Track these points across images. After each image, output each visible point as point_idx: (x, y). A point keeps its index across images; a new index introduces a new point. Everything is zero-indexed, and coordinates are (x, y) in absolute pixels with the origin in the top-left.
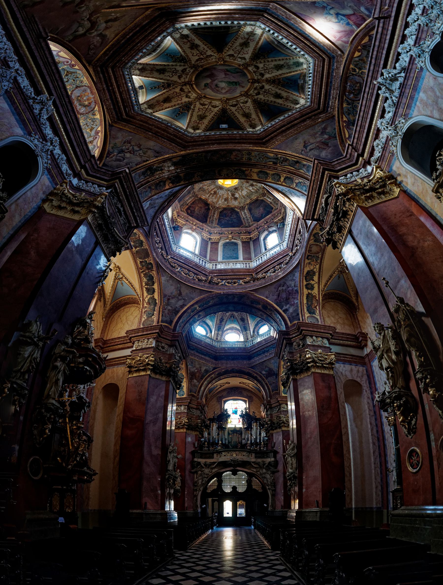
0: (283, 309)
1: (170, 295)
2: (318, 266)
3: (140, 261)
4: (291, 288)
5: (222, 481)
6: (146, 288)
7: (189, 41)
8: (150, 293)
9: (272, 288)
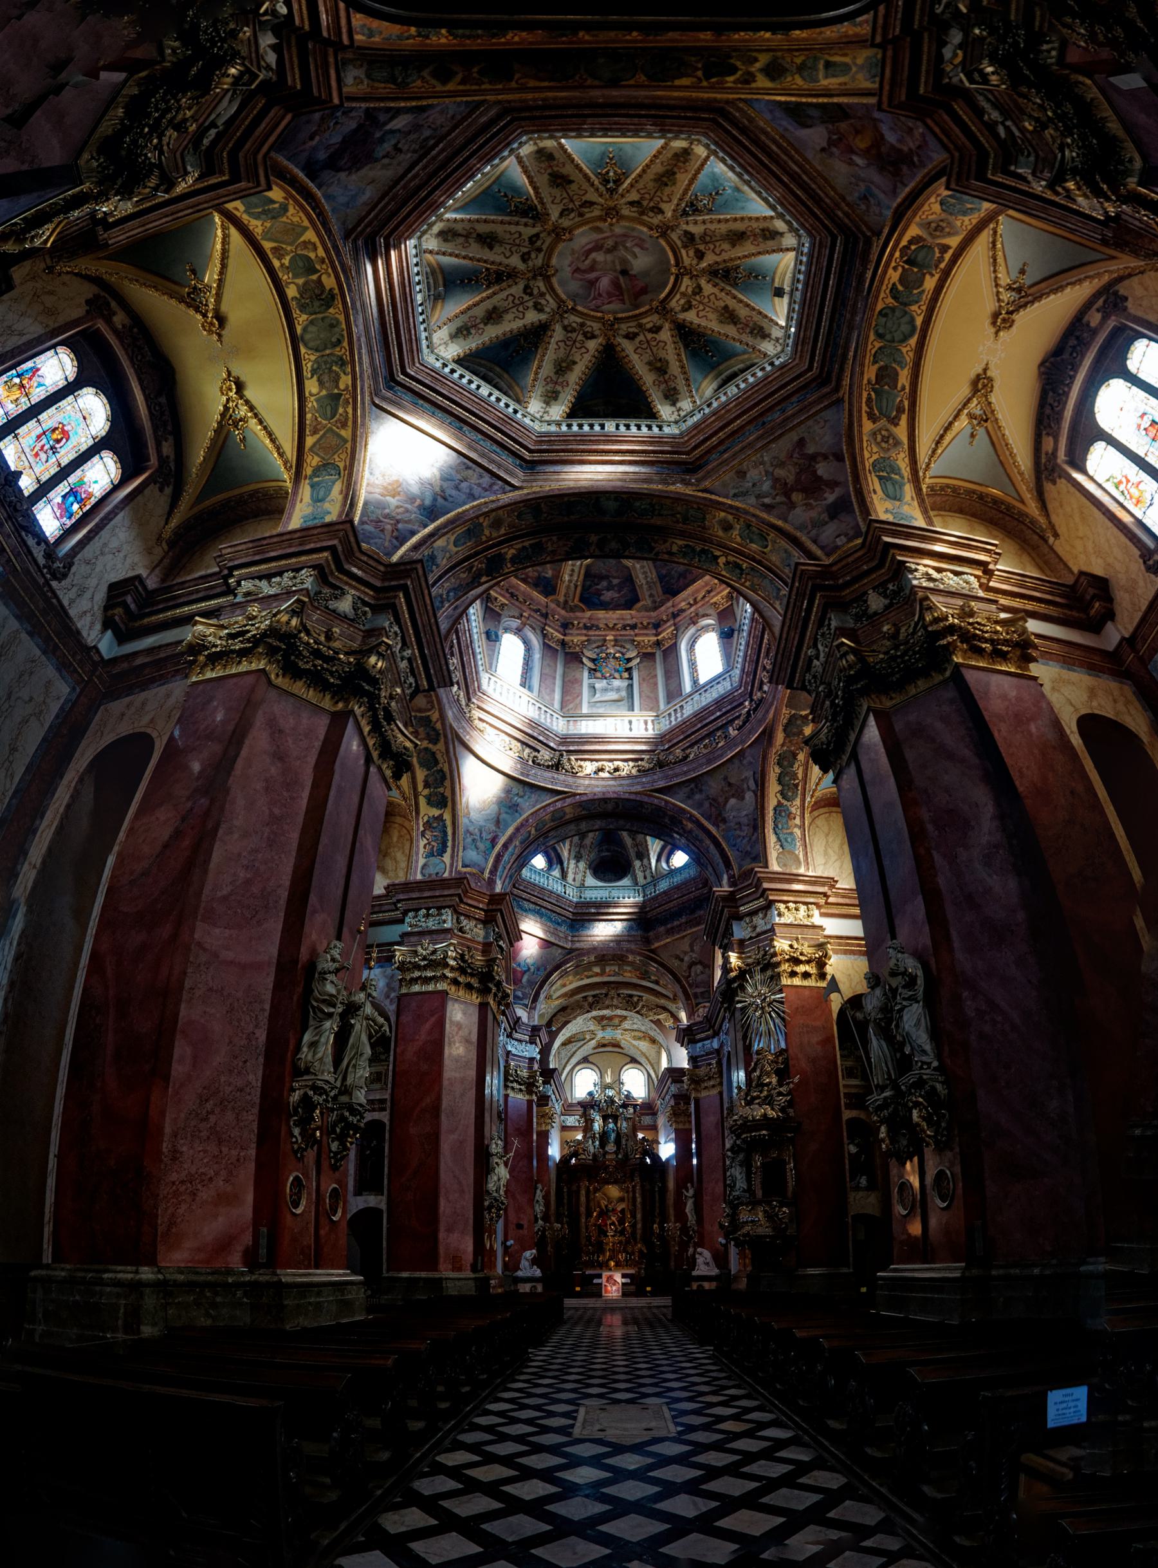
7: (637, 845)
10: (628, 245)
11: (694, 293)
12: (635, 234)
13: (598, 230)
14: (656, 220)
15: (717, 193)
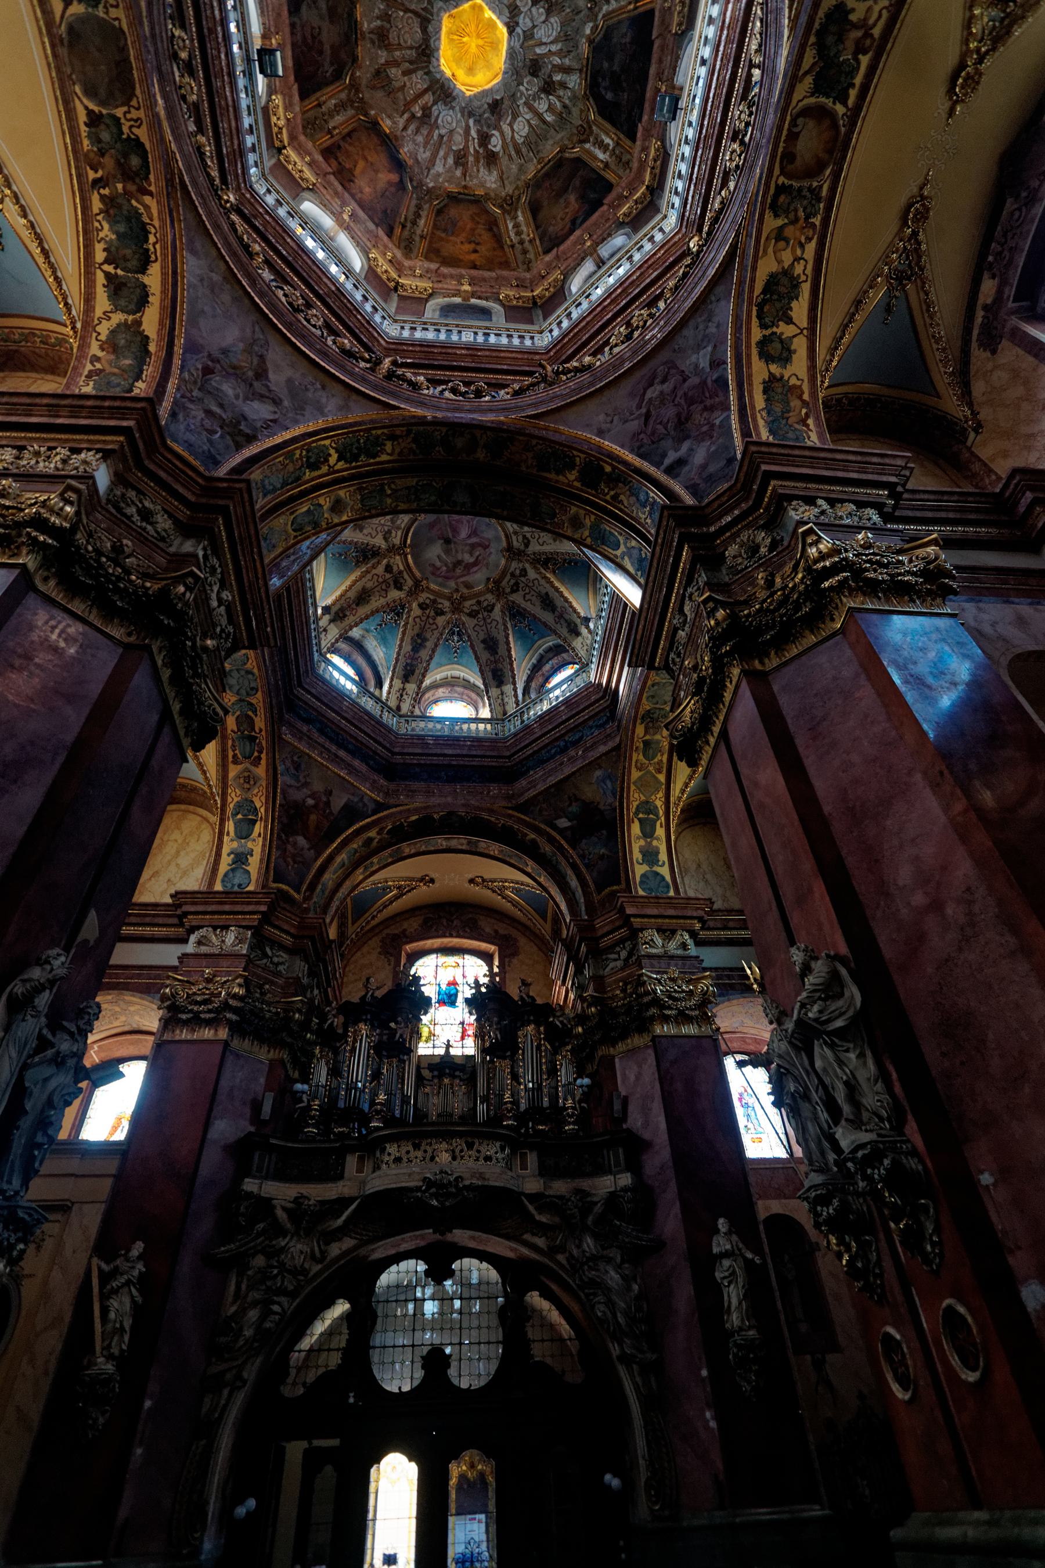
0: (667, 462)
1: (216, 354)
2: (811, 248)
3: (90, 113)
4: (694, 380)
5: (374, 1317)
6: (107, 275)
8: (122, 302)
9: (620, 398)
10: (444, 568)
11: (389, 532)
12: (440, 580)
13: (468, 586)
14: (424, 597)
15: (381, 625)
